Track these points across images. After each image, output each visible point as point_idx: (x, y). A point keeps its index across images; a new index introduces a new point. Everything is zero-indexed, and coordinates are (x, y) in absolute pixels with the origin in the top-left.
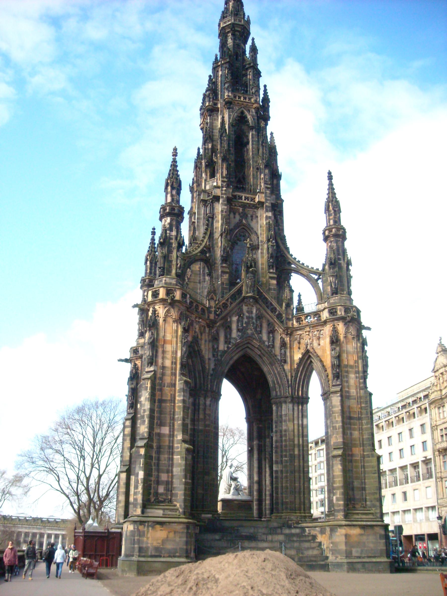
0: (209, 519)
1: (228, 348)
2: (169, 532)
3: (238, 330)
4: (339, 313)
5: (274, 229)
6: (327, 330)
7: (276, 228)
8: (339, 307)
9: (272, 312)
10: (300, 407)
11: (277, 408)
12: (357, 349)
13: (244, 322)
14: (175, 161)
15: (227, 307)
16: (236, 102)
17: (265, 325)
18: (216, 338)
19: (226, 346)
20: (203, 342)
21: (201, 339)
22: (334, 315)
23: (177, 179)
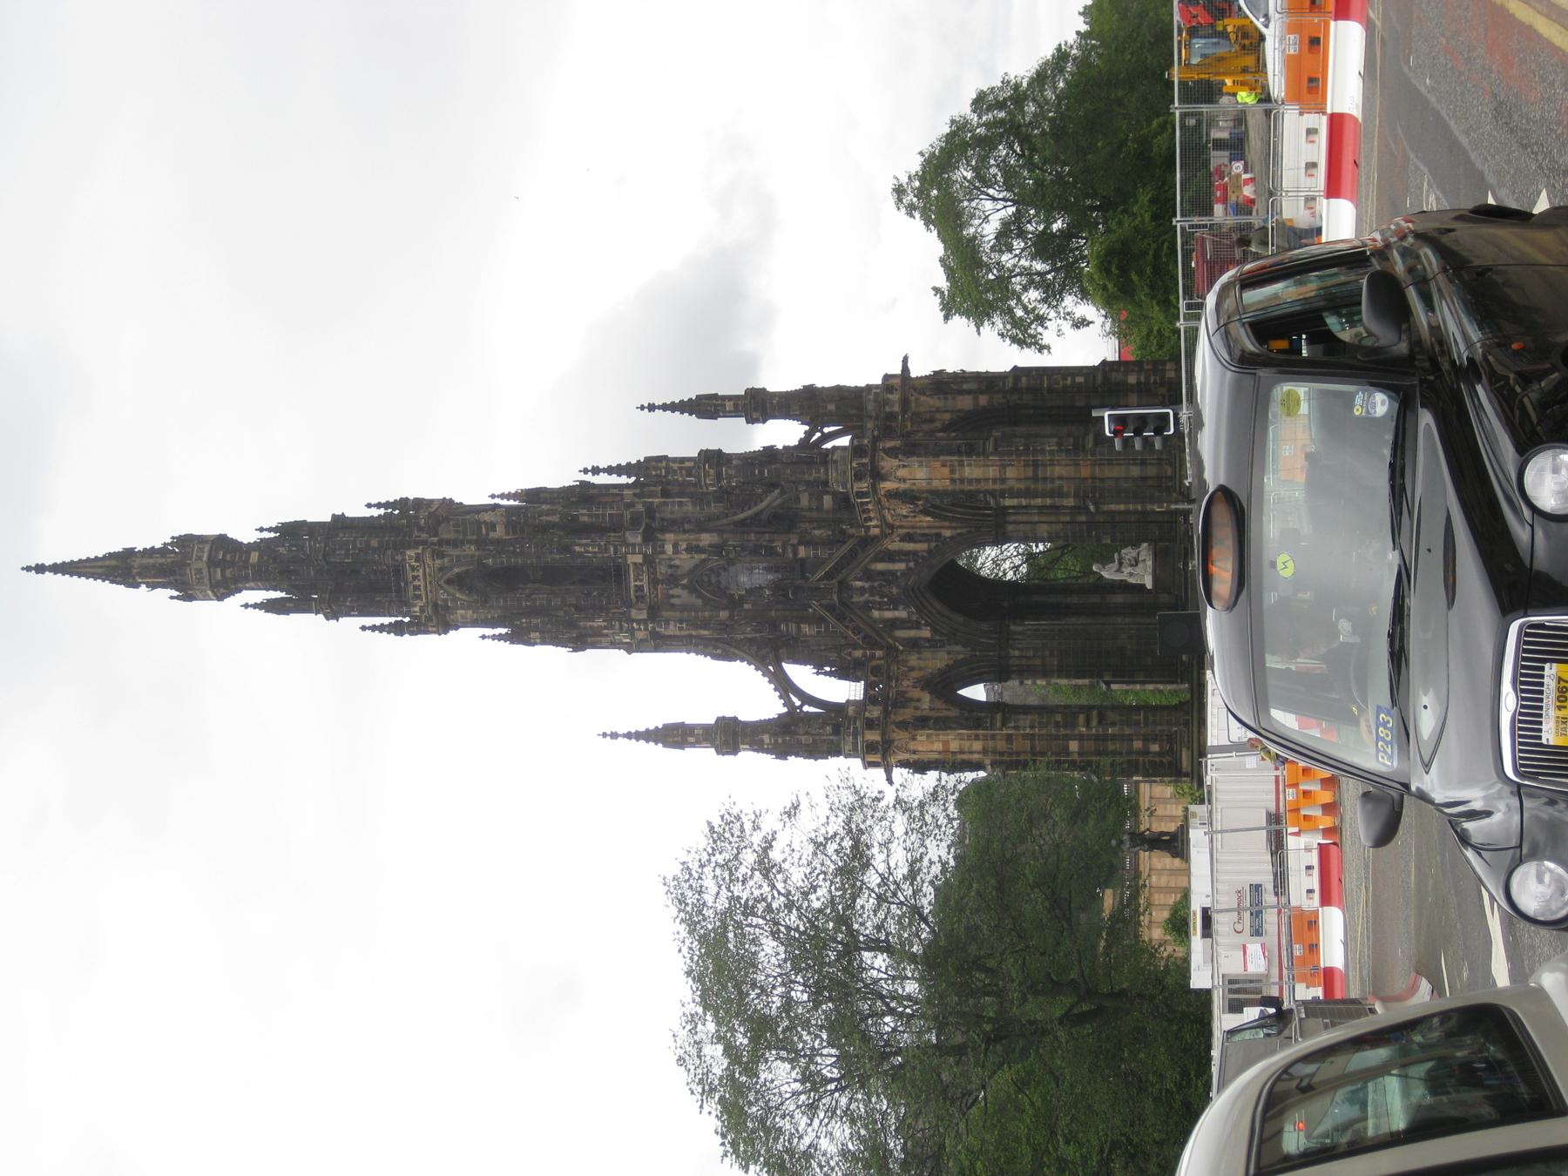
3: (895, 609)
14: (629, 736)
17: (880, 566)
21: (921, 669)
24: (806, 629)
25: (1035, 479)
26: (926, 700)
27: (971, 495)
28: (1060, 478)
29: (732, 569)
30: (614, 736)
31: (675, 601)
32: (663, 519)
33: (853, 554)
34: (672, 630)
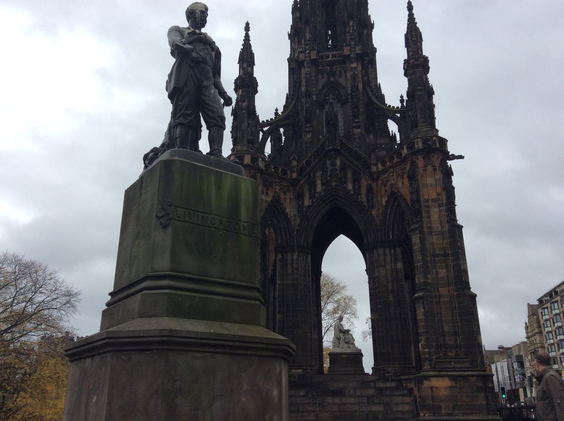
0: (299, 375)
3: (323, 184)
4: (416, 146)
8: (416, 140)
10: (392, 251)
11: (370, 255)
17: (350, 175)
19: (311, 201)
20: (288, 200)
22: (412, 150)
23: (247, 52)
24: (309, 136)
25: (434, 255)
27: (417, 213)
28: (437, 273)
29: (339, 105)
30: (247, 28)
31: (320, 76)
32: (368, 67)
34: (304, 71)
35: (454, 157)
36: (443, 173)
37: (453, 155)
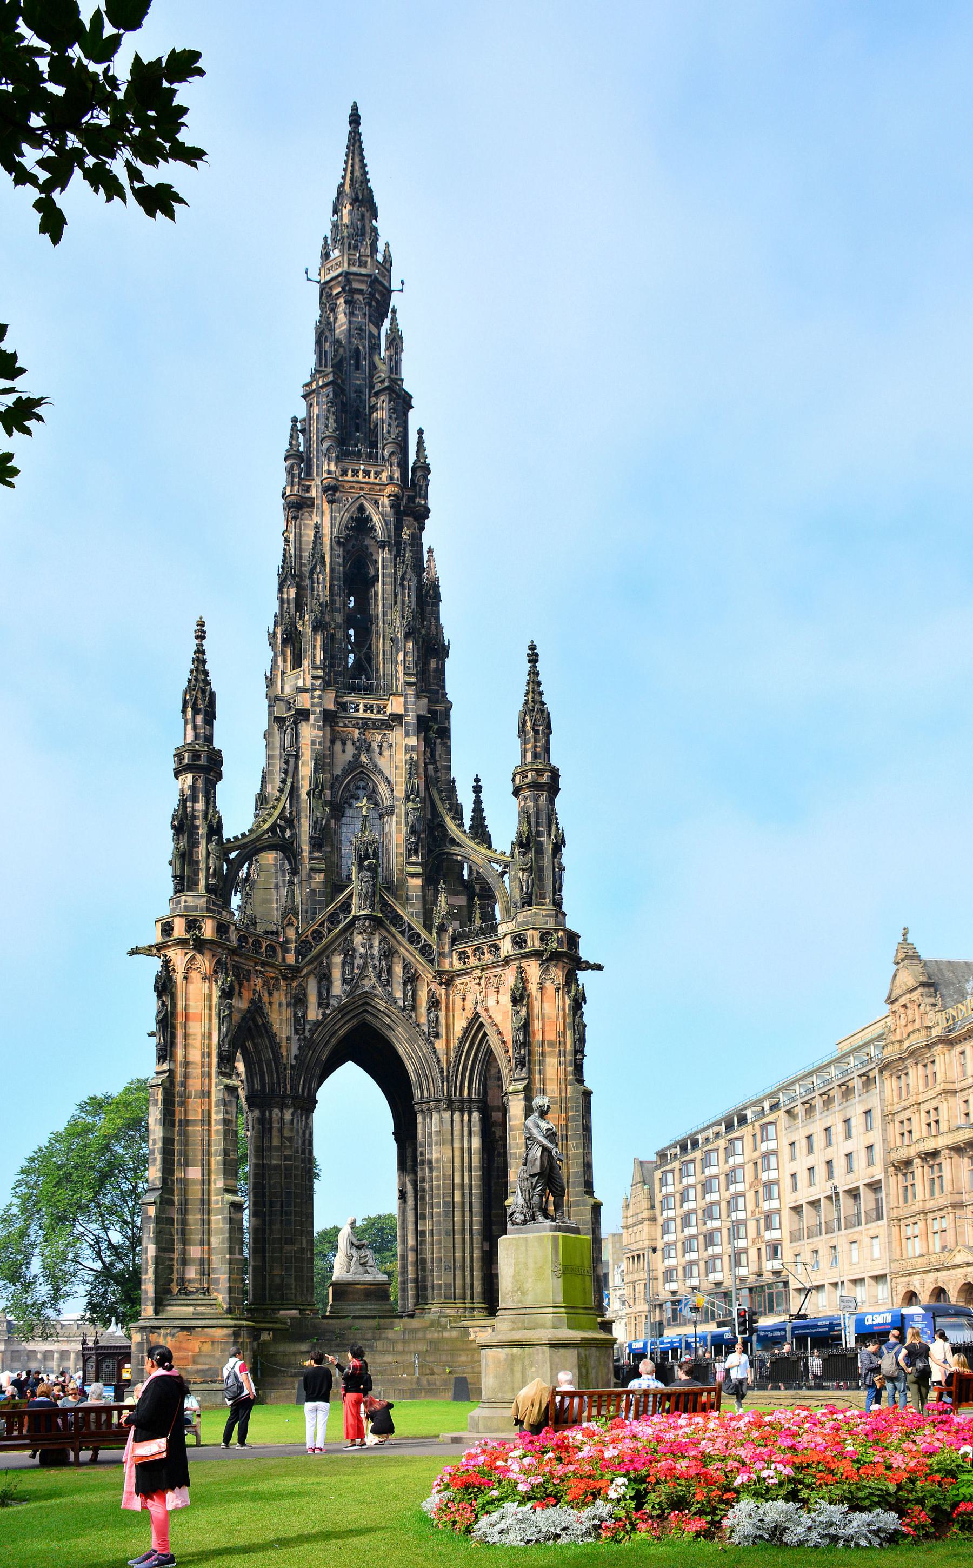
1: (324, 1014)
2: (203, 1343)
3: (344, 981)
4: (529, 943)
5: (426, 770)
6: (510, 976)
7: (431, 767)
8: (529, 932)
9: (412, 943)
12: (564, 1010)
13: (356, 966)
15: (321, 939)
16: (348, 485)
17: (398, 969)
18: (300, 999)
19: (321, 1011)
21: (270, 1003)
22: (521, 947)
26: (241, 1004)
31: (338, 746)
32: (435, 743)
33: (414, 938)
34: (309, 733)
35: (589, 966)
36: (569, 997)
37: (587, 962)
